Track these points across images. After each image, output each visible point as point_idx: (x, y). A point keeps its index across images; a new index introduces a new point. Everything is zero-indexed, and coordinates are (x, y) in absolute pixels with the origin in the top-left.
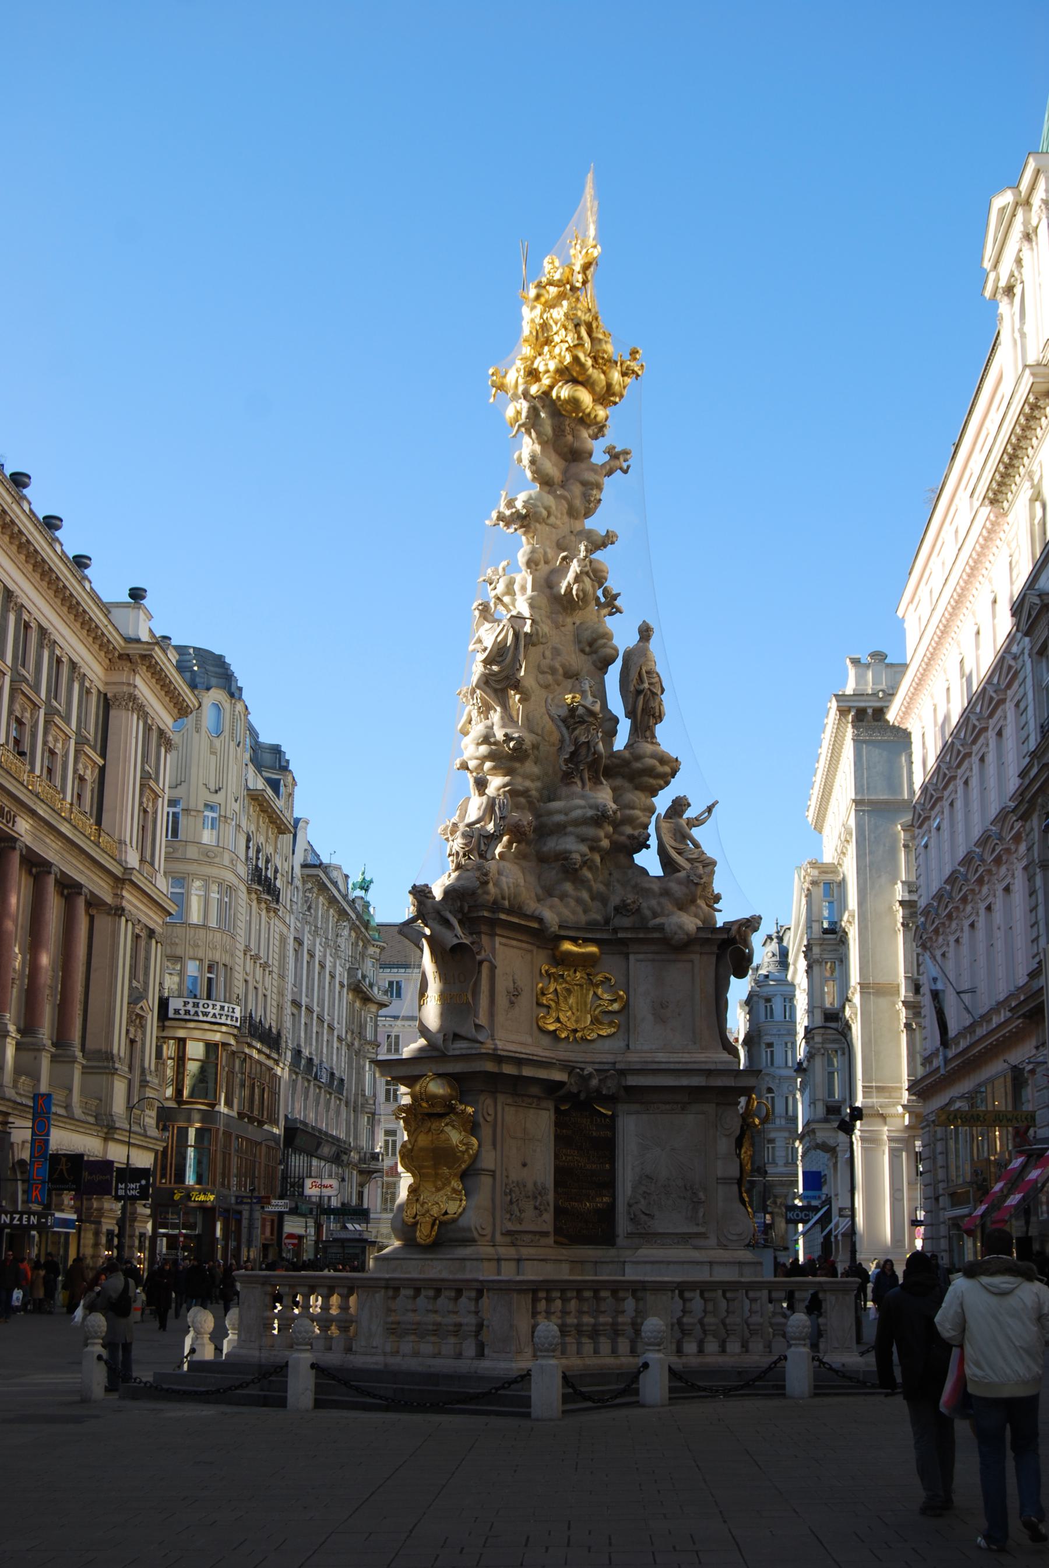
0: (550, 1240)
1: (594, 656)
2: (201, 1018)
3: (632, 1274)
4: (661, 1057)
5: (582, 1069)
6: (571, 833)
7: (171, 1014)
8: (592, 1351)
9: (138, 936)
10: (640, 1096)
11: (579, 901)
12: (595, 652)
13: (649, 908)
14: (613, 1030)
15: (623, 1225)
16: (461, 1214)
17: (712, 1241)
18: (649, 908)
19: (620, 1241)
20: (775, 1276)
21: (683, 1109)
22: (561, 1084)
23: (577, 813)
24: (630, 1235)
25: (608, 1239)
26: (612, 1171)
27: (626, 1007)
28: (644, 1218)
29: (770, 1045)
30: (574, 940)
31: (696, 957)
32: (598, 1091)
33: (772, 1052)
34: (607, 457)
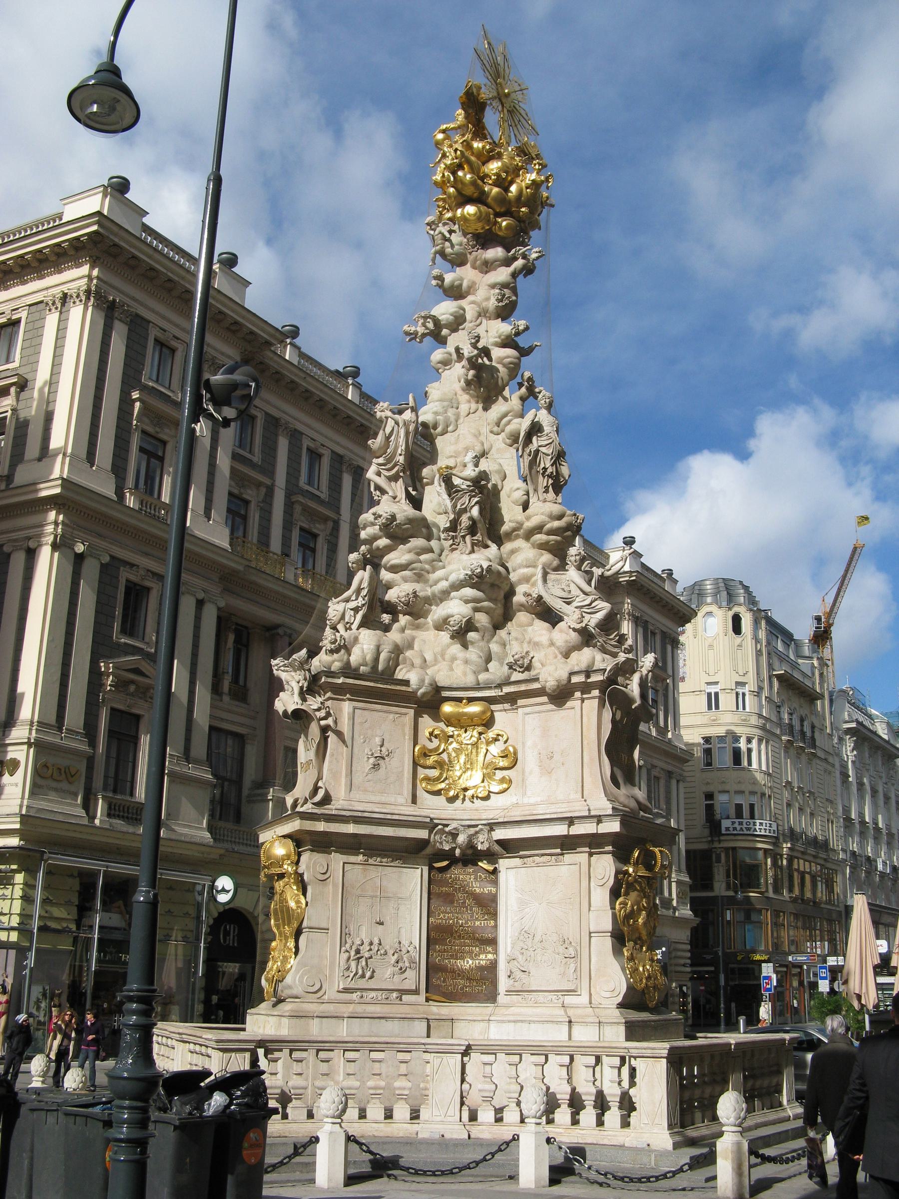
0: (422, 998)
2: (746, 832)
5: (447, 825)
6: (454, 598)
7: (723, 832)
8: (357, 1116)
9: (657, 779)
11: (466, 662)
12: (503, 431)
14: (505, 786)
15: (503, 983)
17: (584, 999)
19: (502, 998)
20: (629, 1038)
22: (424, 843)
23: (453, 578)
25: (491, 997)
26: (496, 926)
30: (459, 700)
32: (471, 845)
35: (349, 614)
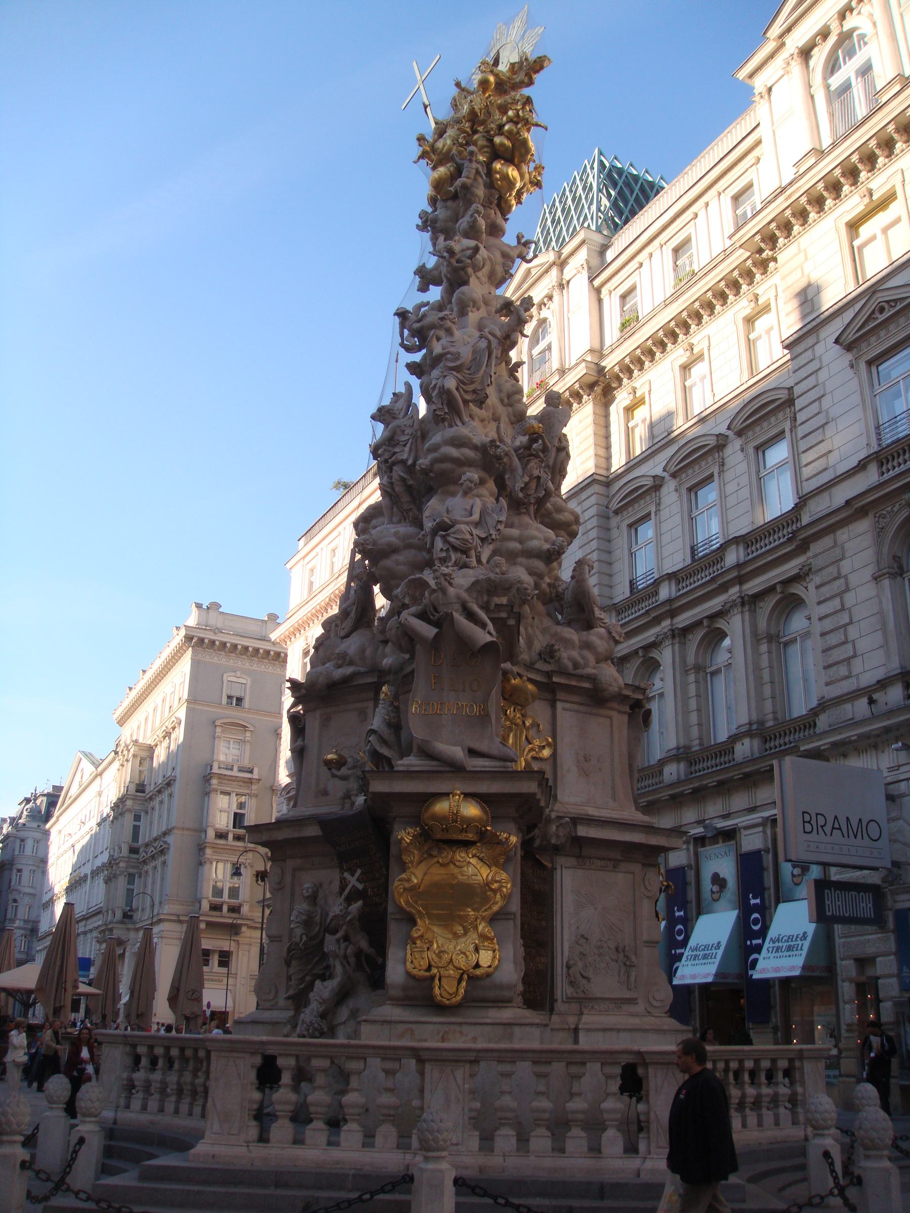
1: (510, 409)
3: (586, 1042)
4: (592, 811)
10: (580, 848)
12: (510, 405)
13: (569, 658)
15: (562, 989)
16: (496, 968)
18: (569, 658)
19: (559, 1006)
21: (615, 867)
23: (534, 544)
24: (569, 1000)
27: (554, 755)
28: (584, 982)
29: (19, 871)
31: (614, 714)
33: (20, 876)
34: (514, 243)
35: (479, 541)
